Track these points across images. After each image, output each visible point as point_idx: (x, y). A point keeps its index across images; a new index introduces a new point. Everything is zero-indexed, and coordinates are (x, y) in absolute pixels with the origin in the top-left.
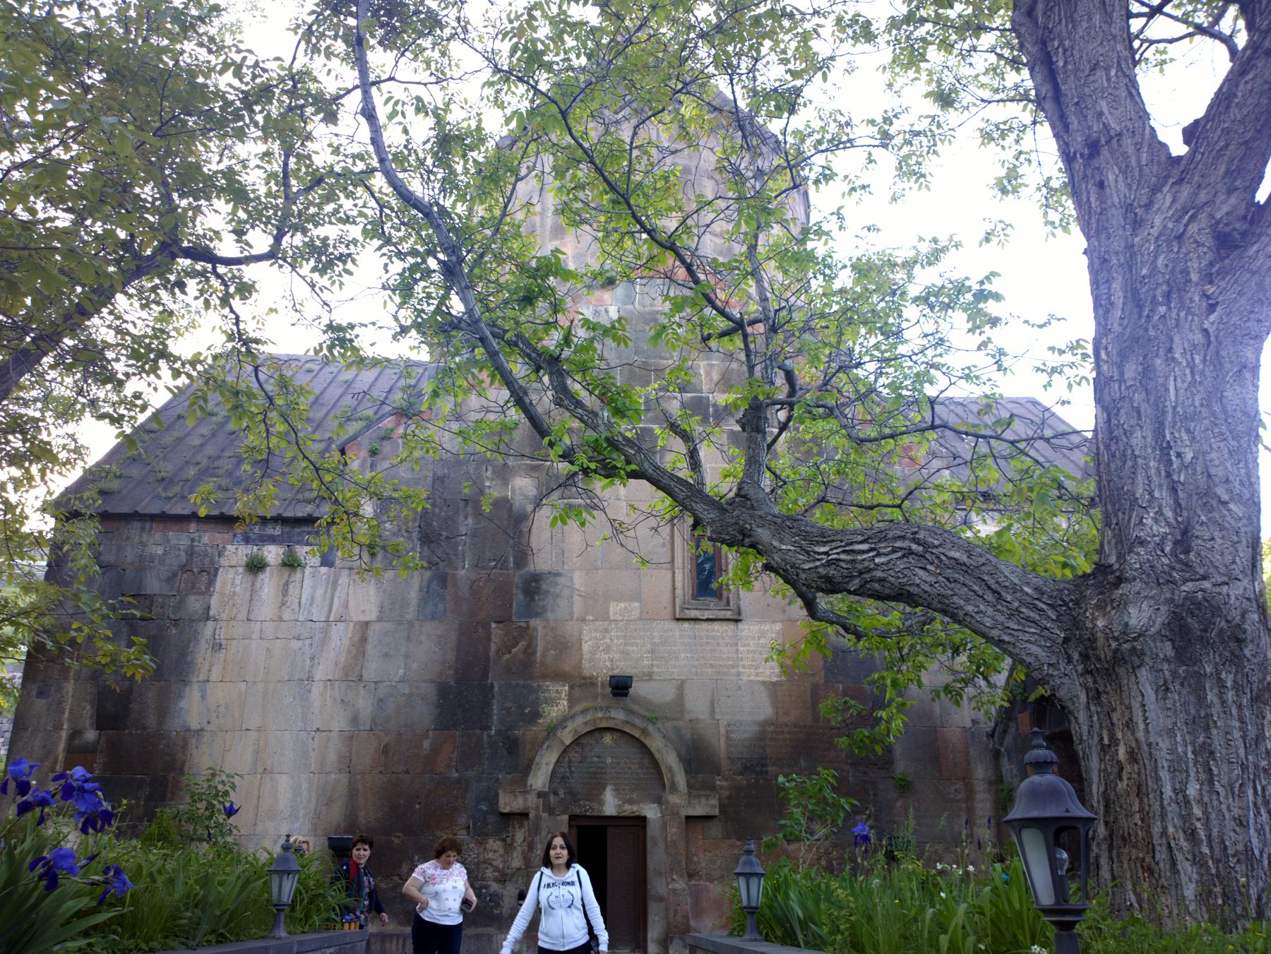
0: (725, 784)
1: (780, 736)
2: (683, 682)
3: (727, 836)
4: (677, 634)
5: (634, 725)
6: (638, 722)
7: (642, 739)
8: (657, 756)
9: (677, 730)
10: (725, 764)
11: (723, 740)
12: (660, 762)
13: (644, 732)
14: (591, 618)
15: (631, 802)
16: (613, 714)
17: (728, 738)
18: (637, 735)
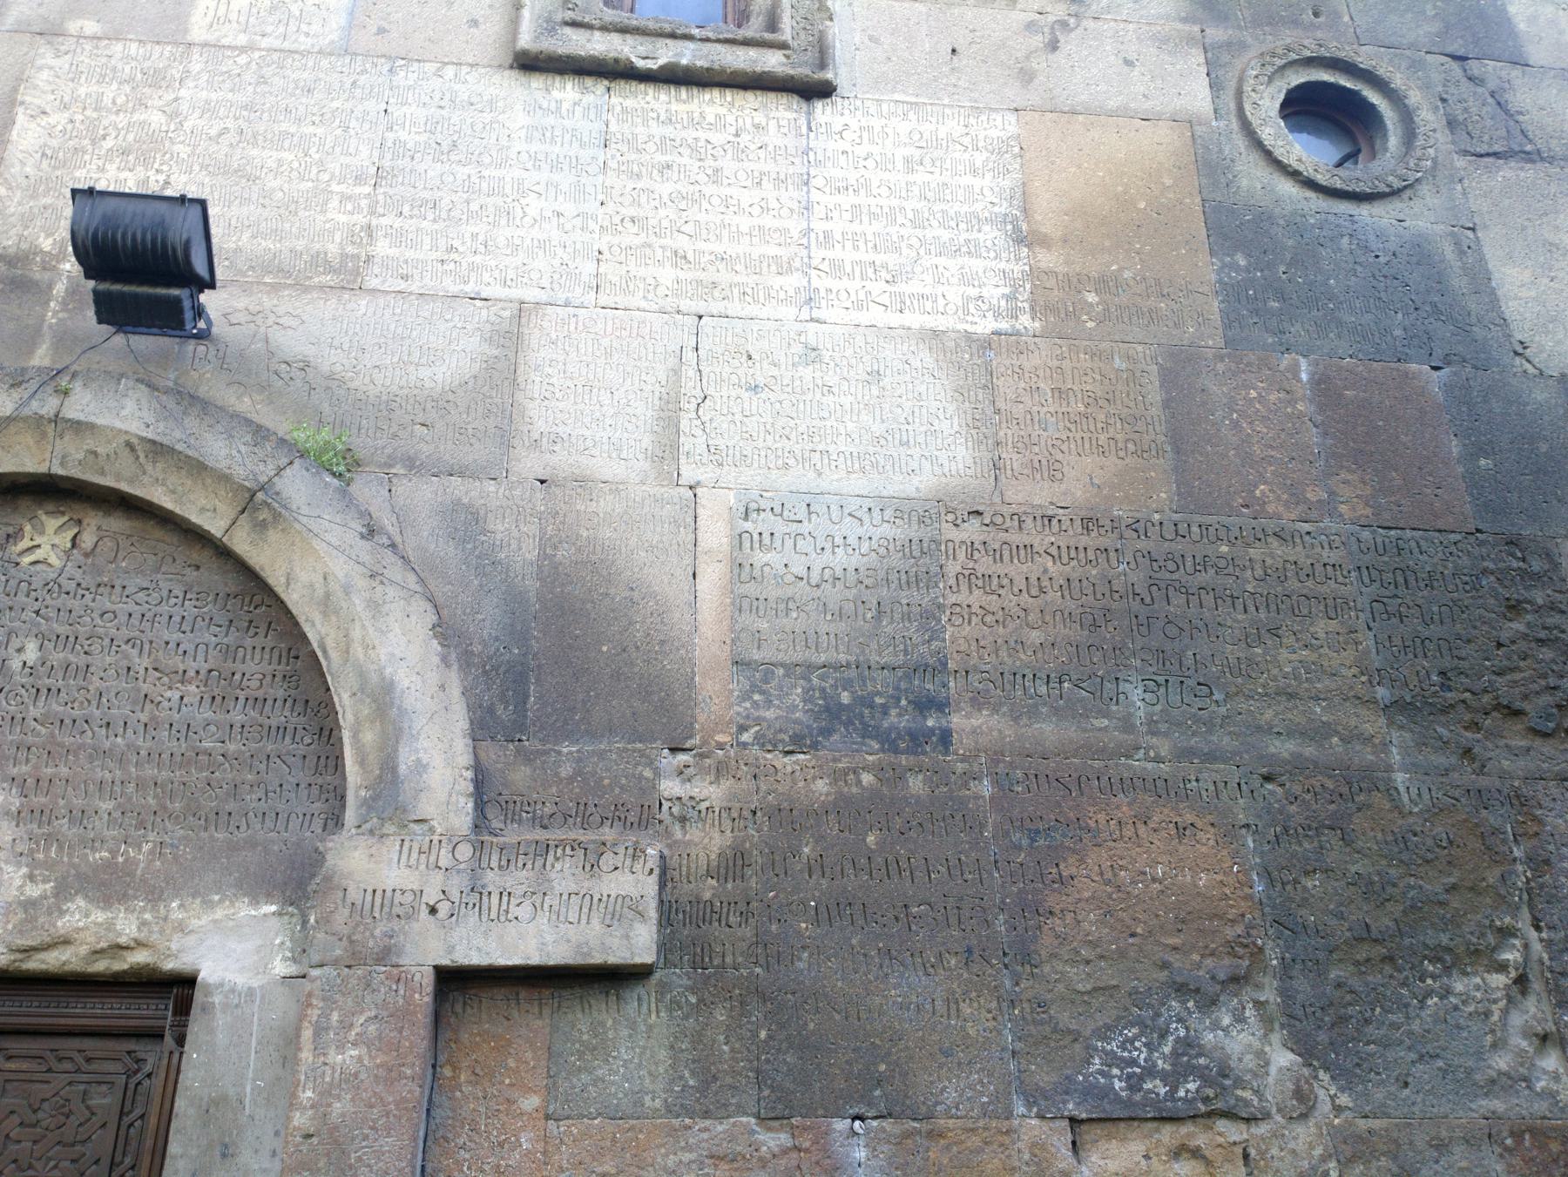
0: (710, 792)
1: (1017, 570)
2: (522, 310)
3: (704, 1095)
4: (518, 119)
5: (198, 468)
6: (219, 450)
7: (241, 543)
8: (316, 629)
9: (466, 524)
10: (715, 696)
11: (712, 577)
12: (332, 663)
13: (254, 502)
14: (91, 27)
15: (109, 886)
16: (82, 404)
17: (739, 568)
18: (215, 526)
